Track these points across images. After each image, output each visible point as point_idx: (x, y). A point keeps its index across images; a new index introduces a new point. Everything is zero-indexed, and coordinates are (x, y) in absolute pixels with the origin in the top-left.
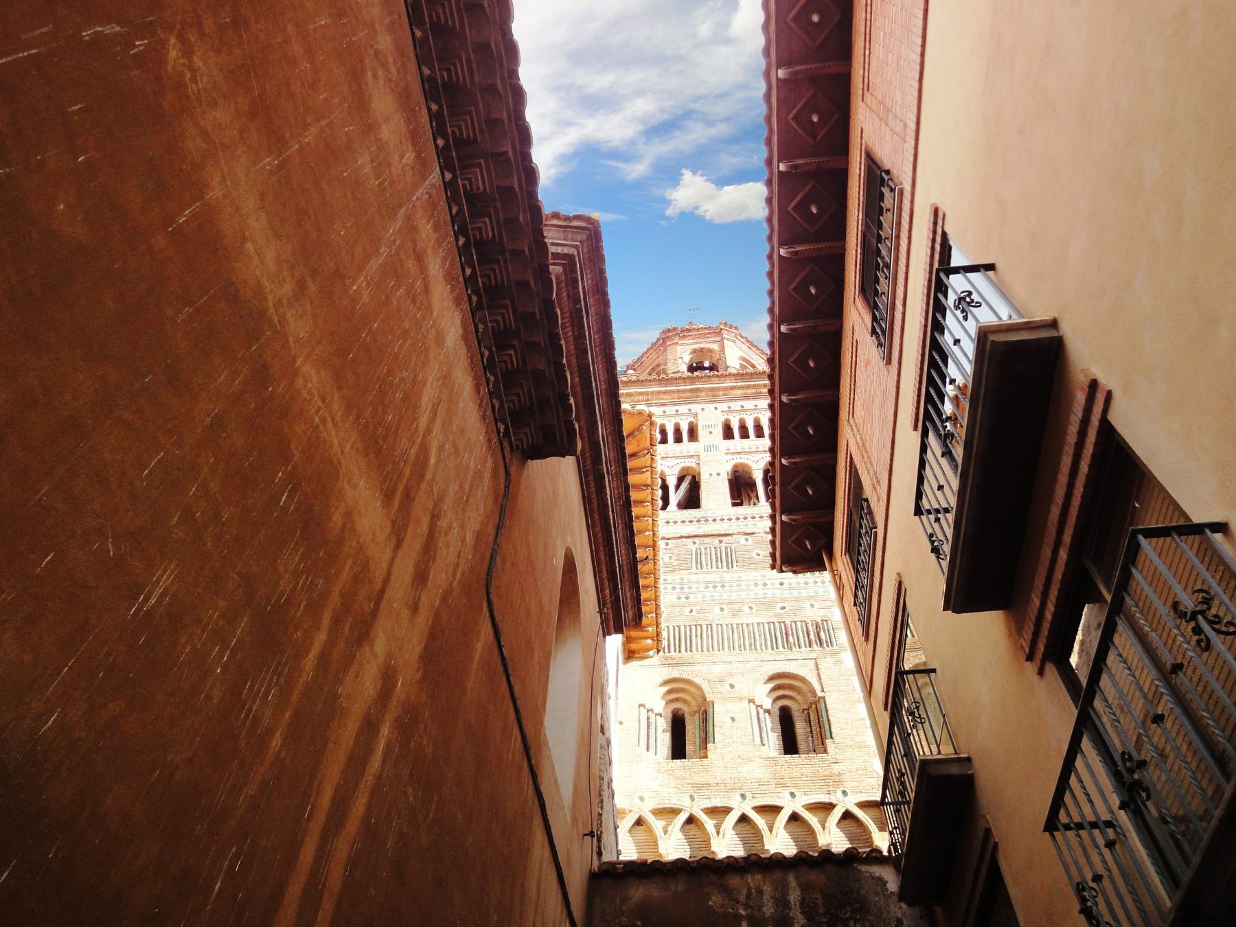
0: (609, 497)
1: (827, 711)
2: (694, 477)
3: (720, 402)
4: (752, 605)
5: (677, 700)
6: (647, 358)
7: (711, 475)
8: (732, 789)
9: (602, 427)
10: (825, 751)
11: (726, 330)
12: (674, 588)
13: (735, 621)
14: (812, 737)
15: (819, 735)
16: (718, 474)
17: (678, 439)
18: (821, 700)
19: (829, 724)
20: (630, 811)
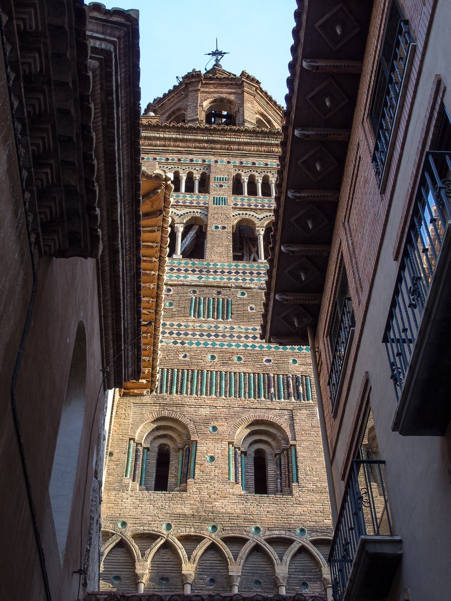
0: (121, 269)
1: (296, 458)
2: (201, 227)
3: (233, 156)
4: (241, 356)
5: (164, 436)
6: (168, 100)
7: (217, 227)
8: (205, 520)
9: (121, 207)
10: (291, 493)
11: (247, 83)
12: (171, 333)
13: (224, 369)
14: (281, 479)
15: (287, 478)
16: (224, 228)
17: (190, 189)
18: (293, 447)
19: (297, 470)
20: (113, 534)
